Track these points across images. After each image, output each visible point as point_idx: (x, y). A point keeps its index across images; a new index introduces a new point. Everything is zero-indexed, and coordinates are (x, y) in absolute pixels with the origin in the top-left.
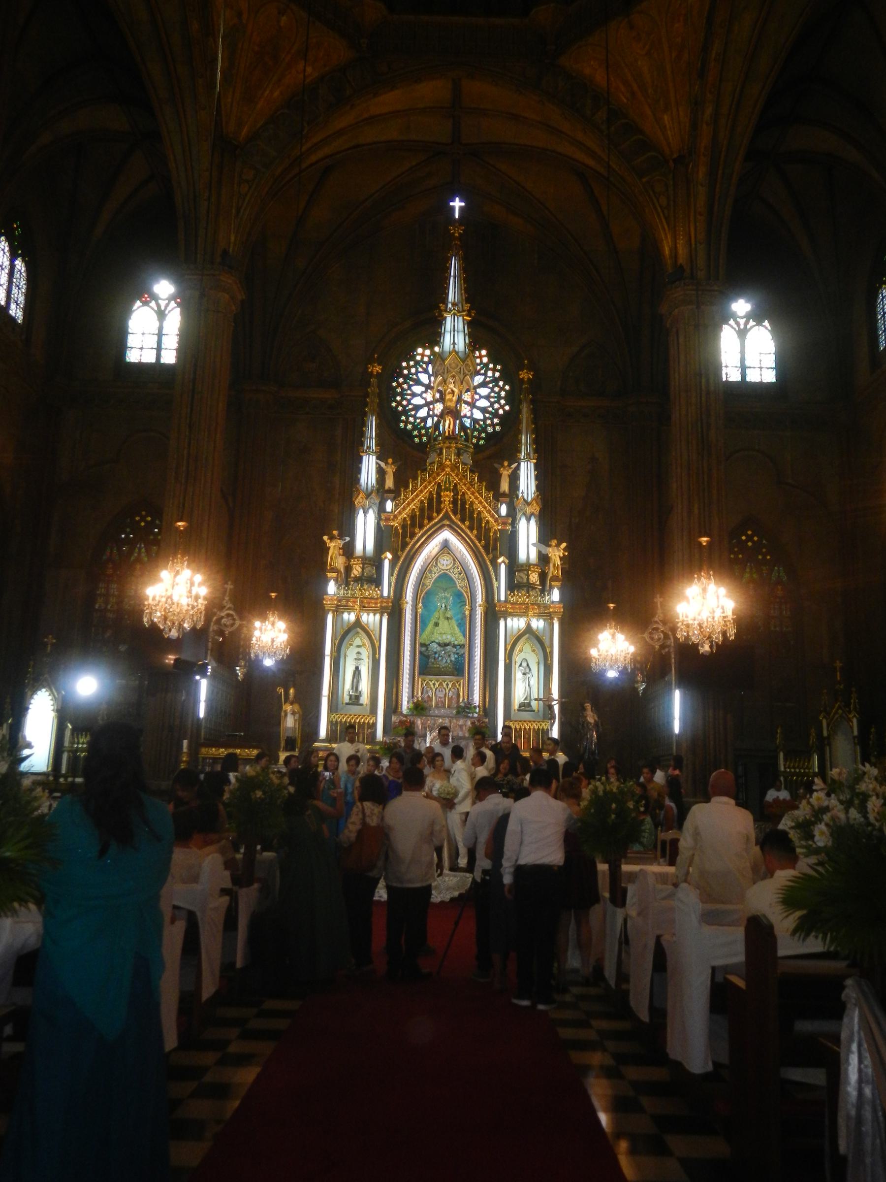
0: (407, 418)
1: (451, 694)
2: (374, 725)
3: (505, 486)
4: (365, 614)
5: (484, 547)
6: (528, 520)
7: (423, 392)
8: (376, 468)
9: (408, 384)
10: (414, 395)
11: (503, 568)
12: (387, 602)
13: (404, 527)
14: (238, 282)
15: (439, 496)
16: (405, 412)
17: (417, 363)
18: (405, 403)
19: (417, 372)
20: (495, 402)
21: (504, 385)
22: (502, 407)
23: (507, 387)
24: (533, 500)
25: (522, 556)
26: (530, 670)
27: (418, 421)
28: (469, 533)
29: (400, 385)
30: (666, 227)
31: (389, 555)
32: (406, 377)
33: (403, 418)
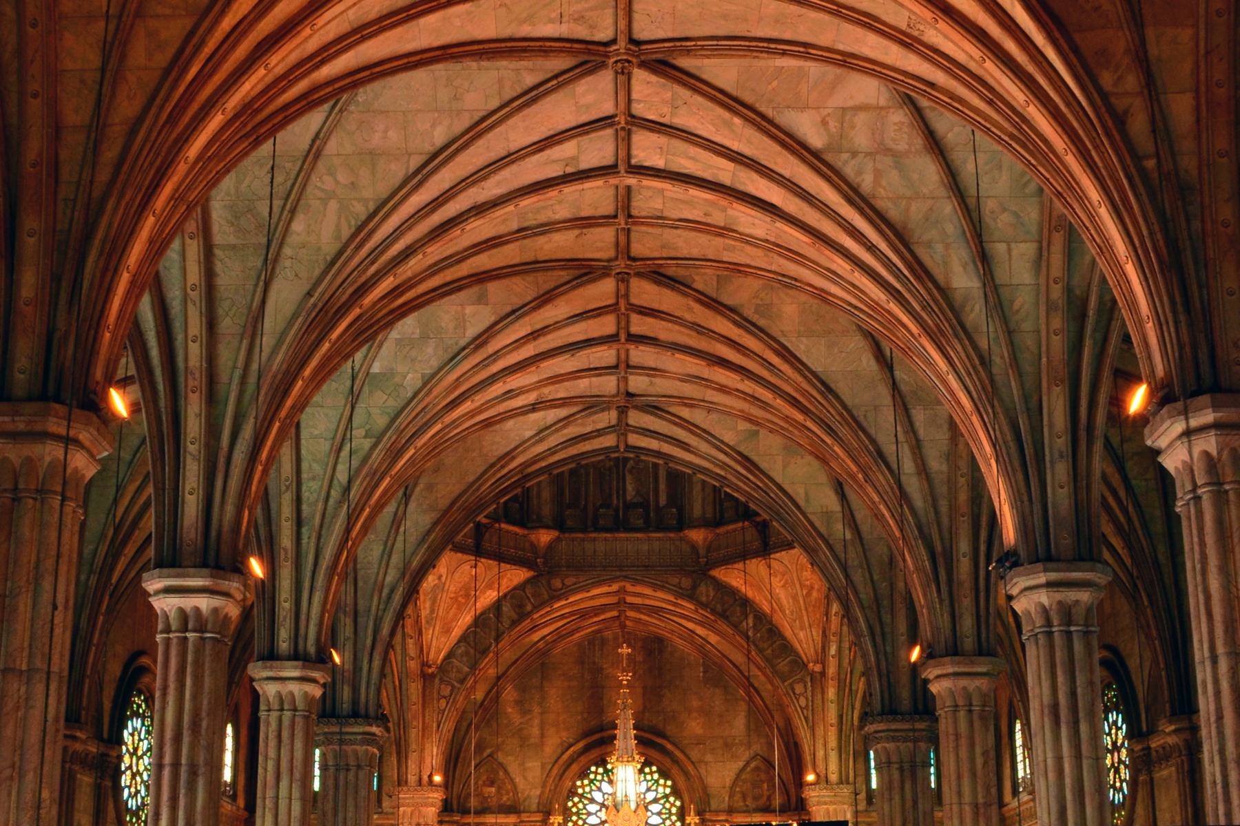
10: (589, 814)
17: (591, 781)
32: (581, 796)
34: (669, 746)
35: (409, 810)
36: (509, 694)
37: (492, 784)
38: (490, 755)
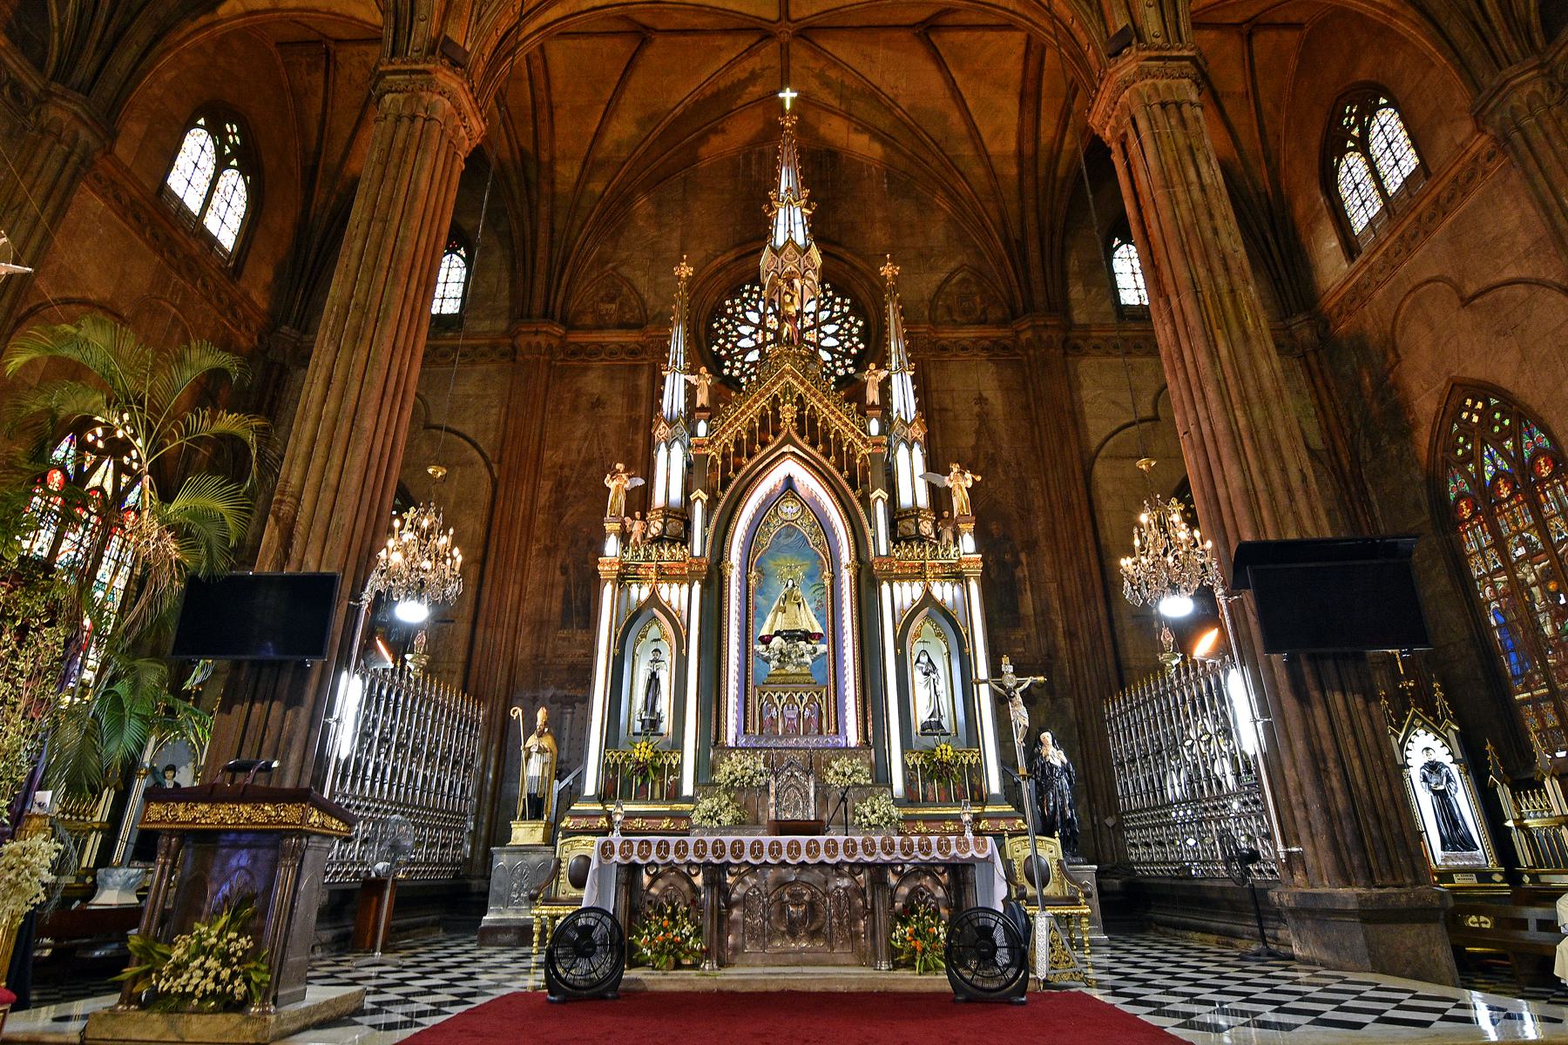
0: (733, 364)
1: (807, 713)
2: (680, 766)
3: (873, 395)
4: (666, 585)
5: (848, 480)
6: (910, 448)
7: (751, 334)
8: (686, 392)
9: (733, 324)
10: (741, 336)
11: (880, 508)
12: (700, 564)
13: (725, 457)
14: (466, 87)
15: (776, 412)
16: (730, 356)
17: (744, 301)
18: (729, 346)
19: (744, 311)
20: (845, 341)
21: (856, 321)
22: (855, 346)
23: (860, 323)
24: (913, 422)
25: (905, 500)
26: (934, 668)
27: (747, 366)
28: (823, 460)
29: (722, 326)
30: (1088, 11)
31: (705, 497)
33: (728, 363)
34: (848, 256)
35: (401, 97)
36: (642, 204)
37: (612, 300)
38: (614, 269)
